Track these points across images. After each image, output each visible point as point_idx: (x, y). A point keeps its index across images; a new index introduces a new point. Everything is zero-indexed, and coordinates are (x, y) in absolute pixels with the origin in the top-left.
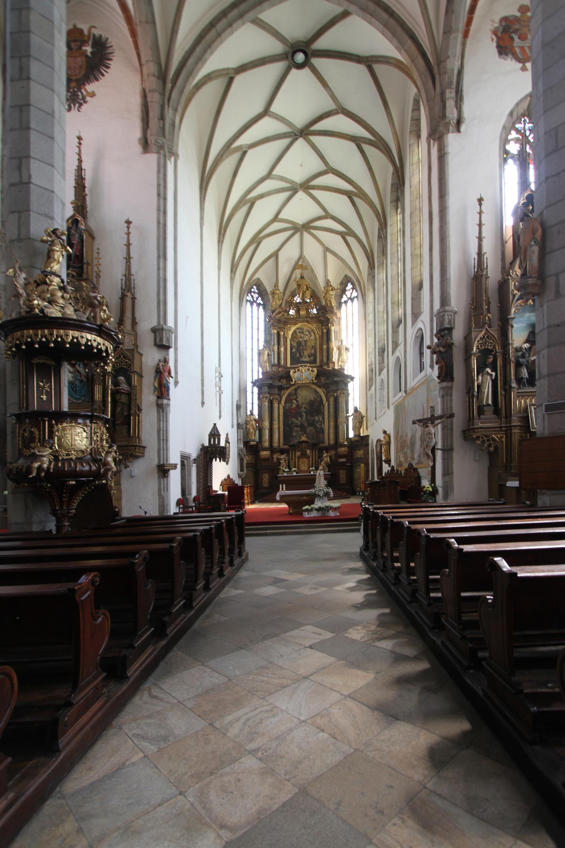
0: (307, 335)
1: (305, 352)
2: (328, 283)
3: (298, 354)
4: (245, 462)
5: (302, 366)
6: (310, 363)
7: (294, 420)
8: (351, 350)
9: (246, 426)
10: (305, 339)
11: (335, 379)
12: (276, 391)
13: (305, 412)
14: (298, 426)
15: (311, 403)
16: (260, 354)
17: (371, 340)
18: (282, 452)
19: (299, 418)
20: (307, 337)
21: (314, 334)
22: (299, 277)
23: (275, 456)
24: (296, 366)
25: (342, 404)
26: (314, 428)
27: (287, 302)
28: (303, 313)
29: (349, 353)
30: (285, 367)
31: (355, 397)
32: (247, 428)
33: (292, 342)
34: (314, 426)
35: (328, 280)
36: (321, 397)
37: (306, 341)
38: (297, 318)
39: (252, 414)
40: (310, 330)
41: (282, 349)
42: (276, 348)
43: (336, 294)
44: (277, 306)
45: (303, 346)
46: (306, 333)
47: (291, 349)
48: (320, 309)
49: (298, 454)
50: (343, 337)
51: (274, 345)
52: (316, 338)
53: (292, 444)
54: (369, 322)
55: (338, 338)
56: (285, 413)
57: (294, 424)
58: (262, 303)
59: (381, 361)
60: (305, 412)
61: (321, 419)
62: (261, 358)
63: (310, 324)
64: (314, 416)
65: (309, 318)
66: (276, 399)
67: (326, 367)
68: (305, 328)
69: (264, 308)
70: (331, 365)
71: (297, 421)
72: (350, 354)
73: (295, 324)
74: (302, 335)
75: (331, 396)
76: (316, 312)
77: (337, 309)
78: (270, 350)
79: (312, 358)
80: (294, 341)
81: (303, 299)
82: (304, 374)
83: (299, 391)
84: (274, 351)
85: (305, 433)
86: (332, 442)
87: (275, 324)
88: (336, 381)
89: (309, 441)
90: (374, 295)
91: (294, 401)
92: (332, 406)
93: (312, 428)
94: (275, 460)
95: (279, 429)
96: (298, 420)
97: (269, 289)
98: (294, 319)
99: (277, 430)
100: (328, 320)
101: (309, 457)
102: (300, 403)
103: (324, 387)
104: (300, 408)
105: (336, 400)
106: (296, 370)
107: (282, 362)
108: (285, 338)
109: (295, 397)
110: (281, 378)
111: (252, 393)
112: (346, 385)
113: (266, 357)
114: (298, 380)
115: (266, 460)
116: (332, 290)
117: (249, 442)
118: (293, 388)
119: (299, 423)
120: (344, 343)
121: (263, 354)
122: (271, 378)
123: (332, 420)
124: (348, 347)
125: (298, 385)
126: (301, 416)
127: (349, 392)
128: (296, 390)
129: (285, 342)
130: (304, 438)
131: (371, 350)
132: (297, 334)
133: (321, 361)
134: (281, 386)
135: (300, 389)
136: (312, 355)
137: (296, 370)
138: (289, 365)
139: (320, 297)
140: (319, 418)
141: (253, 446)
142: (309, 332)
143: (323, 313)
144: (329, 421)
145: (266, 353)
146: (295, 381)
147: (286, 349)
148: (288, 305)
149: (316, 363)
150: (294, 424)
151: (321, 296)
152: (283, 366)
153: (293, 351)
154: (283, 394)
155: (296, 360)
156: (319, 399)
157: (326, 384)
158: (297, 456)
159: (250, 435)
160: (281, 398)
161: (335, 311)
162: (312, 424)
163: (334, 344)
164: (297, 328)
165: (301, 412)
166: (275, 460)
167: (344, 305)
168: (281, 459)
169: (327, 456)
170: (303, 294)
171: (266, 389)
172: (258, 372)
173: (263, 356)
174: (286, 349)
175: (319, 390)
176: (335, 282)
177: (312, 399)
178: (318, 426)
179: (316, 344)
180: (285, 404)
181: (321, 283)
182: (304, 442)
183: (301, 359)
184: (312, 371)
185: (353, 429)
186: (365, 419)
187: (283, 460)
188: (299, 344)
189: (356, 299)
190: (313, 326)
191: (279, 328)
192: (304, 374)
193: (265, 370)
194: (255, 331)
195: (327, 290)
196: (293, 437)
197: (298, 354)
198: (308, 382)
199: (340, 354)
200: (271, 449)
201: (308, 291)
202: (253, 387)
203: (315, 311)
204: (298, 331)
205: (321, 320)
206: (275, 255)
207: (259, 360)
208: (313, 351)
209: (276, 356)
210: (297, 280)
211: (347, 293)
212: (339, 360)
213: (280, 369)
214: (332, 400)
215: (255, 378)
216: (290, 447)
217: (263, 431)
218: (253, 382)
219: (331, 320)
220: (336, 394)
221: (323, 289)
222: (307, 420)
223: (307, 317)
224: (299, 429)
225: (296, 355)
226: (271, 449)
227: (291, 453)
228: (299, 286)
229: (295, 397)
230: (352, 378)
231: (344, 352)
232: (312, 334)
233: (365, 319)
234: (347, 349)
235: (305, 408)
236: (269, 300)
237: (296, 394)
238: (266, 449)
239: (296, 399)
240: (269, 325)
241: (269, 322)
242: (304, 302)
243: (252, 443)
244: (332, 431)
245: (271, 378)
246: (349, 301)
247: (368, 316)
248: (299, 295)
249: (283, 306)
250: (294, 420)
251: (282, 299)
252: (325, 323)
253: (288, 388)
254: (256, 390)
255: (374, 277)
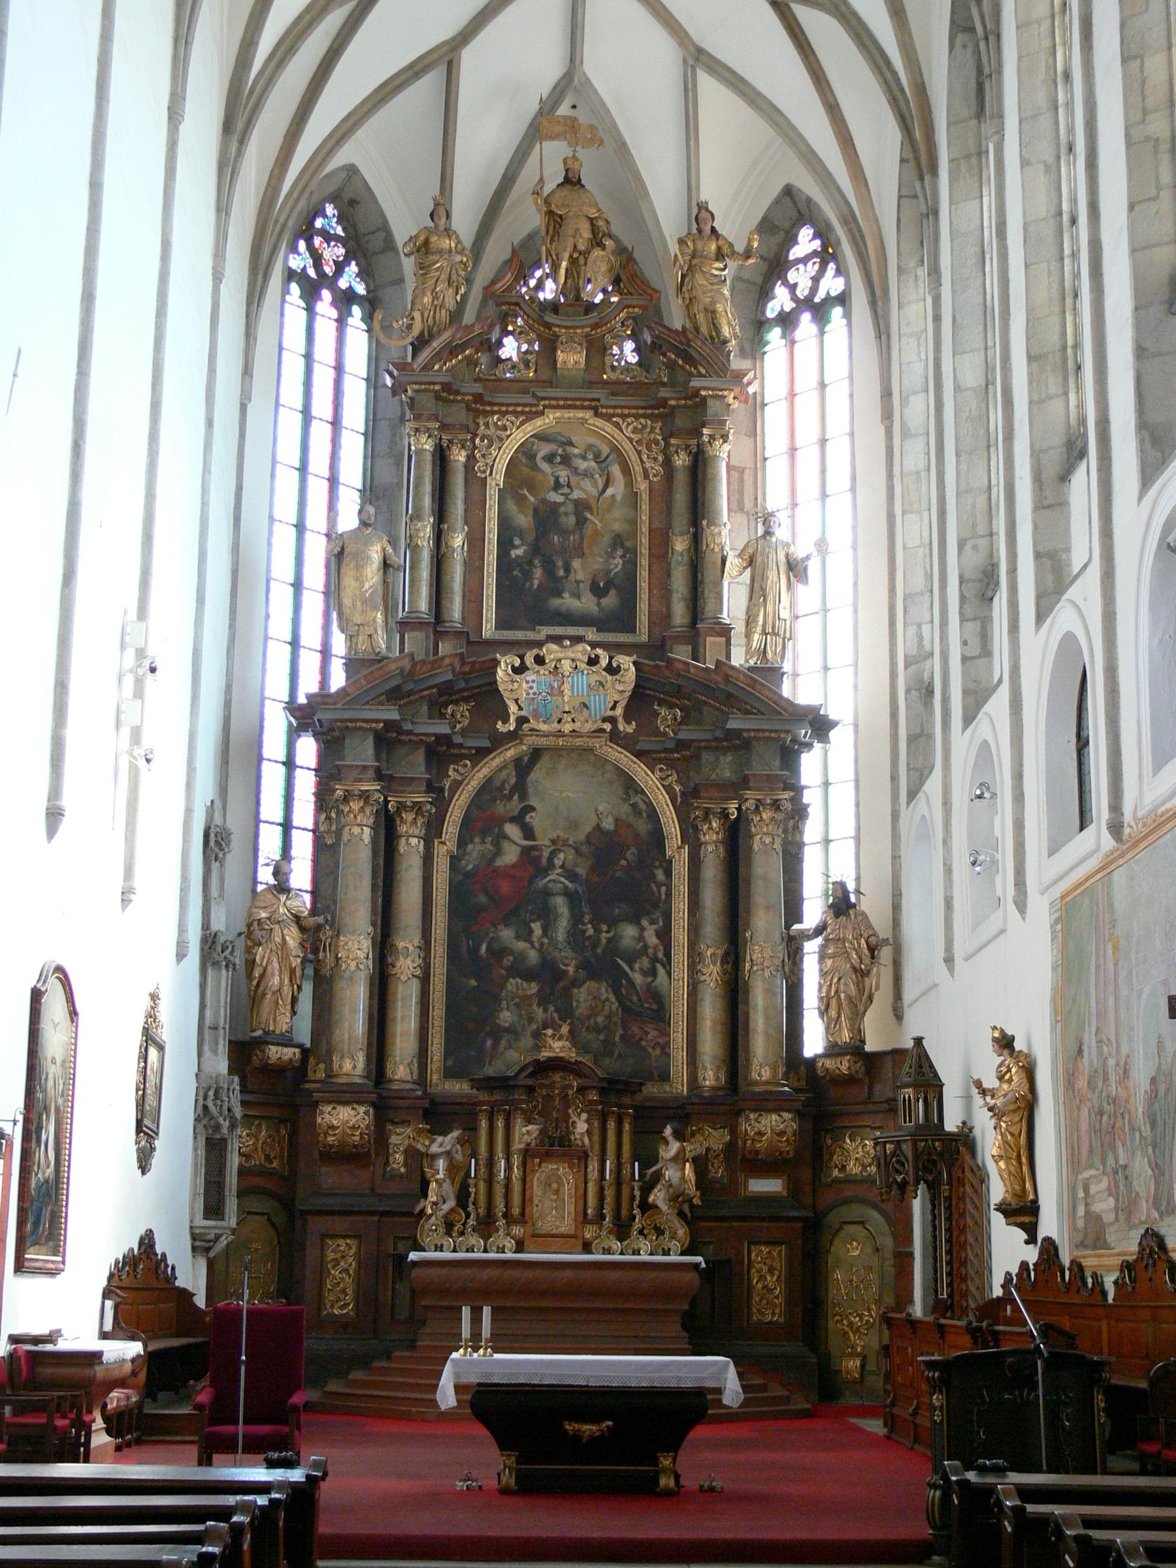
0: (587, 474)
1: (576, 564)
2: (700, 218)
3: (538, 573)
4: (234, 1161)
5: (557, 639)
6: (601, 624)
7: (507, 934)
8: (813, 568)
9: (249, 950)
10: (576, 494)
11: (732, 725)
12: (416, 765)
13: (566, 893)
14: (529, 976)
15: (604, 847)
16: (340, 556)
17: (915, 531)
18: (437, 1114)
19: (537, 927)
20: (587, 485)
21: (626, 471)
22: (555, 176)
23: (400, 1138)
24: (531, 635)
25: (765, 867)
26: (616, 992)
27: (488, 292)
28: (571, 358)
29: (800, 588)
30: (470, 639)
31: (834, 833)
32: (251, 964)
33: (511, 506)
34: (617, 980)
35: (702, 207)
36: (653, 815)
37: (582, 507)
38: (537, 381)
39: (282, 887)
40: (605, 450)
41: (458, 540)
42: (426, 530)
43: (737, 279)
44: (443, 315)
45: (565, 533)
46: (583, 465)
47: (504, 545)
48: (655, 347)
49: (526, 1132)
50: (775, 498)
51: (417, 516)
52: (633, 497)
53: (490, 1071)
54: (906, 434)
55: (748, 504)
56: (457, 892)
57: (508, 961)
58: (360, 289)
59: (974, 649)
60: (566, 893)
61: (652, 940)
62: (349, 582)
63: (608, 418)
64: (613, 923)
65: (599, 391)
66: (418, 808)
67: (681, 653)
68: (581, 440)
69: (368, 318)
70: (712, 644)
71: (522, 945)
72: (807, 595)
73: (530, 416)
74: (563, 474)
75: (707, 813)
76: (633, 358)
77: (743, 354)
78: (393, 542)
79: (611, 601)
80: (521, 500)
81: (571, 289)
82: (565, 686)
83: (536, 775)
84: (414, 548)
85: (566, 1013)
86: (710, 1077)
87: (427, 401)
88: (738, 733)
89: (586, 1059)
90: (937, 301)
91: (512, 830)
92: (712, 871)
93: (604, 991)
94: (398, 1160)
95: (425, 980)
96: (527, 936)
97: (404, 223)
98: (523, 387)
99: (414, 987)
100: (698, 404)
101: (584, 1157)
102: (543, 840)
103: (671, 764)
104: (545, 872)
105: (736, 838)
106: (529, 660)
107: (455, 610)
108: (476, 483)
109: (515, 805)
110: (443, 697)
111: (290, 764)
112: (789, 756)
113: (372, 574)
114: (536, 715)
115: (348, 1156)
116: (720, 256)
117: (261, 1043)
118: (511, 753)
119: (533, 956)
120: (781, 533)
121: (361, 560)
122: (394, 695)
123: (712, 949)
124: (799, 552)
125: (531, 741)
126: (547, 916)
127: (807, 797)
128: (524, 767)
129: (475, 505)
130: (558, 1047)
131: (919, 583)
132: (535, 467)
133: (661, 619)
134: (444, 740)
135: (545, 759)
136: (610, 584)
137: (529, 660)
138: (489, 629)
139: (655, 283)
140: (641, 938)
141: (280, 1070)
142: (597, 457)
143: (671, 366)
144: (695, 958)
145: (375, 554)
146: (522, 720)
147: (476, 542)
148: (492, 311)
149: (632, 630)
150: (508, 961)
151: (667, 280)
152: (458, 634)
153: (514, 553)
154: (457, 785)
155: (529, 603)
156: (643, 827)
157: (681, 745)
158: (517, 1145)
159: (266, 1007)
160: (442, 804)
161: (737, 363)
162: (604, 966)
163: (729, 534)
164: (540, 437)
165: (547, 893)
166: (398, 1160)
167: (774, 335)
168: (434, 1157)
169: (679, 1159)
170: (573, 261)
171: (362, 752)
172: (326, 652)
173: (359, 567)
174: (476, 542)
175: (648, 779)
176: (736, 223)
177: (608, 824)
178: (638, 978)
179: (634, 523)
180: (462, 842)
181: (669, 217)
182: (556, 1064)
183: (555, 603)
184: (612, 670)
185: (824, 1012)
186: (885, 954)
187: (441, 1164)
188: (546, 517)
189: (837, 312)
190: (621, 434)
191: (444, 427)
192: (565, 686)
193: (363, 645)
194: (321, 433)
195: (694, 255)
196: (497, 1033)
197: (538, 573)
198: (589, 727)
199: (757, 591)
200: (377, 1091)
201: (597, 253)
202: (293, 734)
203: (629, 352)
204: (544, 449)
205: (663, 403)
206: (444, 60)
207: (332, 593)
208: (617, 563)
209: (425, 573)
210: (548, 188)
211: (792, 276)
212: (750, 621)
213: (445, 648)
214: (712, 835)
215: (309, 685)
216: (480, 1094)
217: (341, 984)
218: (291, 707)
219: (713, 406)
220: (732, 807)
221: (674, 248)
222: (576, 938)
223: (591, 384)
224: (533, 988)
225: (528, 575)
226: (377, 1091)
227: (484, 1124)
228: (555, 221)
229: (515, 805)
230: (821, 726)
231: (777, 579)
232: (616, 470)
233: (887, 416)
234: (795, 569)
235: (571, 875)
236: (401, 281)
237: (521, 788)
238: (347, 1095)
239: (518, 820)
240: (392, 407)
241: (395, 390)
242: (573, 301)
243: (275, 1053)
244: (711, 1011)
245: (394, 695)
246: (806, 317)
247: (904, 402)
248: (555, 268)
249: (469, 317)
250: (507, 934)
251: (469, 281)
252: (680, 422)
253: (481, 754)
254: (308, 749)
255: (934, 212)
